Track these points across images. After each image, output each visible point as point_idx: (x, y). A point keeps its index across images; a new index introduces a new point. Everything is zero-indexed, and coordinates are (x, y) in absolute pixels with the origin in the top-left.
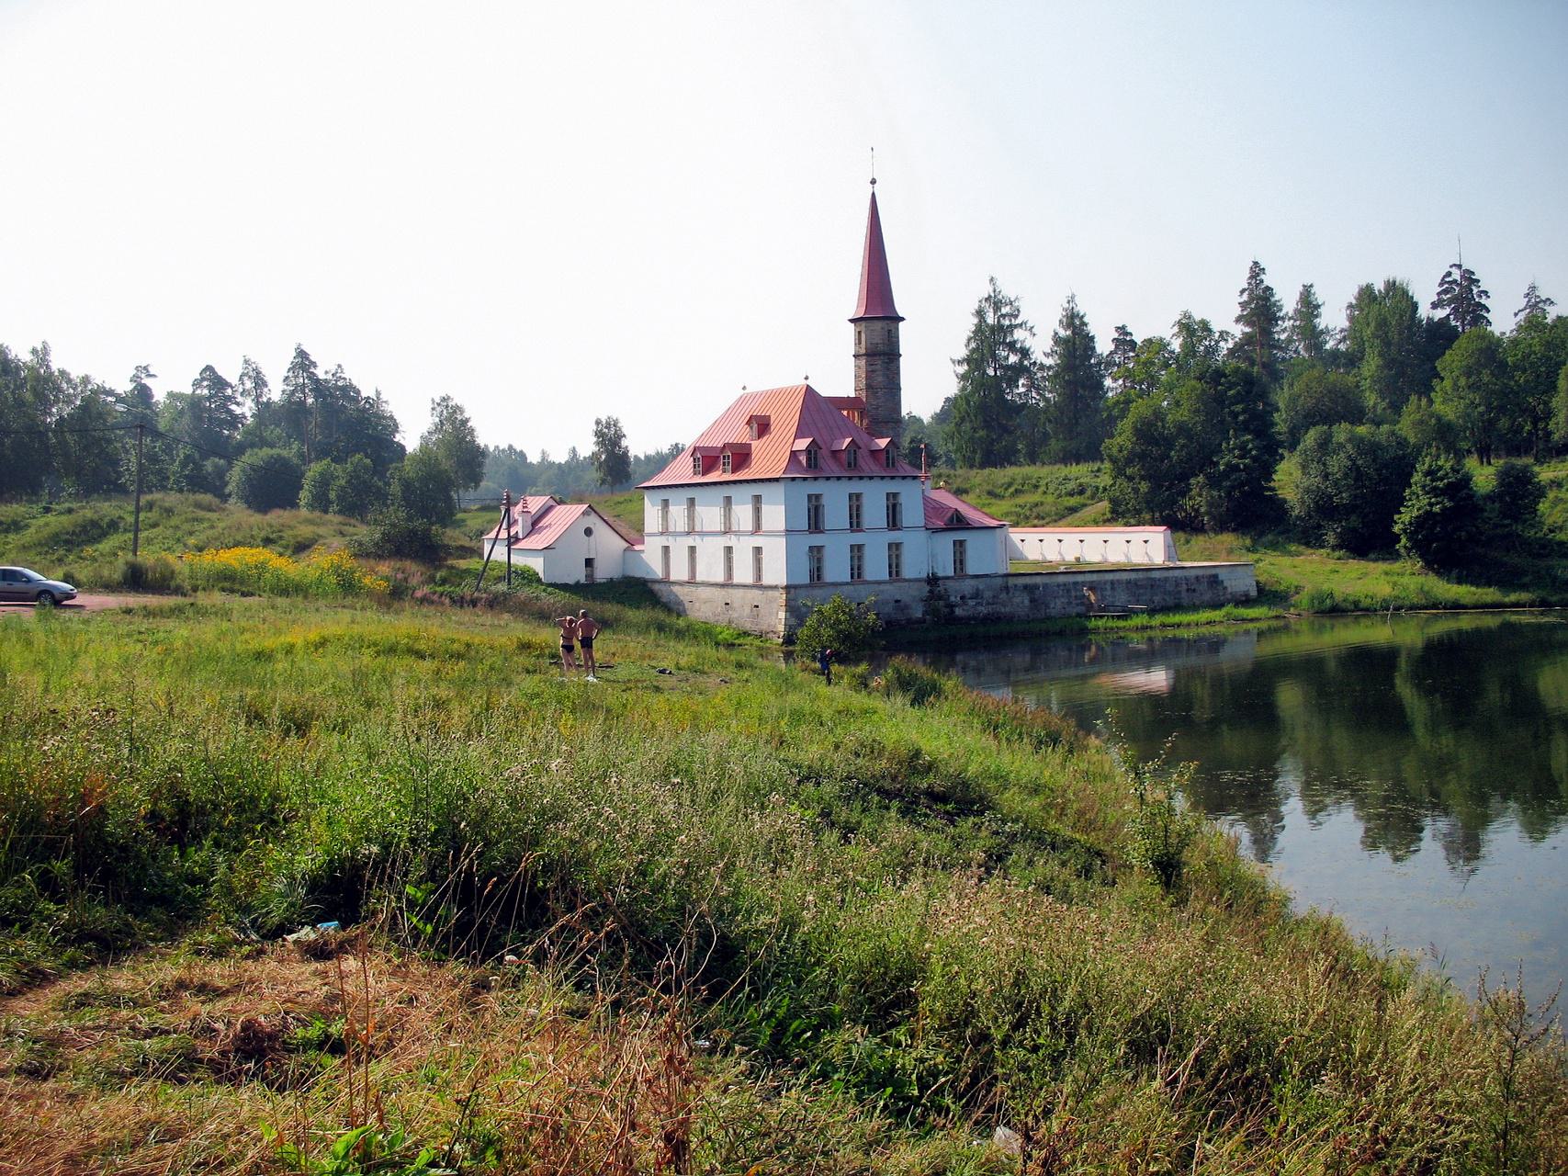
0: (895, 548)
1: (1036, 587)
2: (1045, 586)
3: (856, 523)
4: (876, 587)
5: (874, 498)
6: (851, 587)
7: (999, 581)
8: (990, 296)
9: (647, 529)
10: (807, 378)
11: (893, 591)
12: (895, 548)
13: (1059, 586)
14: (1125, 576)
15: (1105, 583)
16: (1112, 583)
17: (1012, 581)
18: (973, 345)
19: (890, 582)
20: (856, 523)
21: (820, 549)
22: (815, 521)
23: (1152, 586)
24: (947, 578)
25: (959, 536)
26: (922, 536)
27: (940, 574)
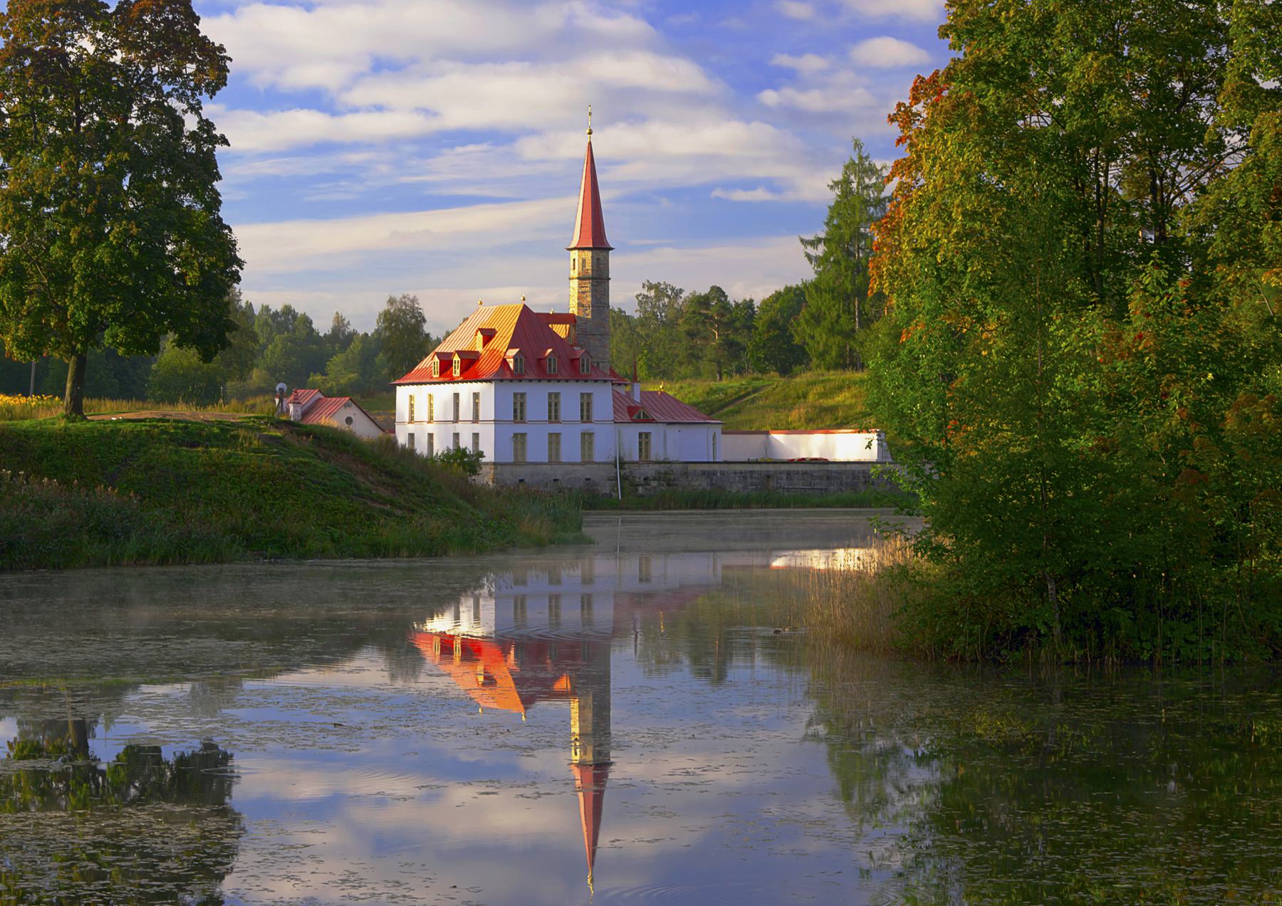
0: (587, 438)
1: (714, 473)
2: (723, 473)
3: (554, 416)
5: (570, 395)
6: (549, 467)
11: (583, 472)
12: (587, 438)
14: (801, 468)
16: (789, 473)
17: (691, 467)
20: (554, 416)
21: (523, 435)
22: (519, 414)
23: (828, 478)
24: (633, 463)
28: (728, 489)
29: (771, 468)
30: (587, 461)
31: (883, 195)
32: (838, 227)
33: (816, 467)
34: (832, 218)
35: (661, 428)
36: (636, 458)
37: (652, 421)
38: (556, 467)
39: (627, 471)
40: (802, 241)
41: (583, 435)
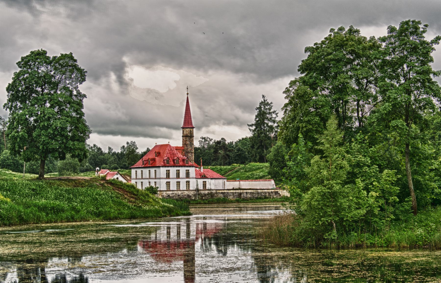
0: (188, 182)
1: (225, 193)
2: (227, 193)
4: (183, 192)
5: (183, 171)
7: (214, 191)
8: (262, 102)
9: (132, 177)
10: (169, 142)
11: (186, 193)
12: (188, 182)
13: (231, 193)
15: (244, 192)
16: (246, 193)
18: (257, 119)
19: (187, 190)
21: (169, 182)
24: (201, 190)
25: (205, 180)
26: (195, 180)
27: (200, 189)
28: (229, 197)
29: (241, 191)
30: (188, 189)
31: (271, 111)
32: (257, 121)
33: (254, 191)
34: (256, 118)
35: (209, 180)
36: (202, 188)
37: (207, 178)
38: (179, 192)
39: (200, 192)
40: (248, 125)
41: (187, 182)
